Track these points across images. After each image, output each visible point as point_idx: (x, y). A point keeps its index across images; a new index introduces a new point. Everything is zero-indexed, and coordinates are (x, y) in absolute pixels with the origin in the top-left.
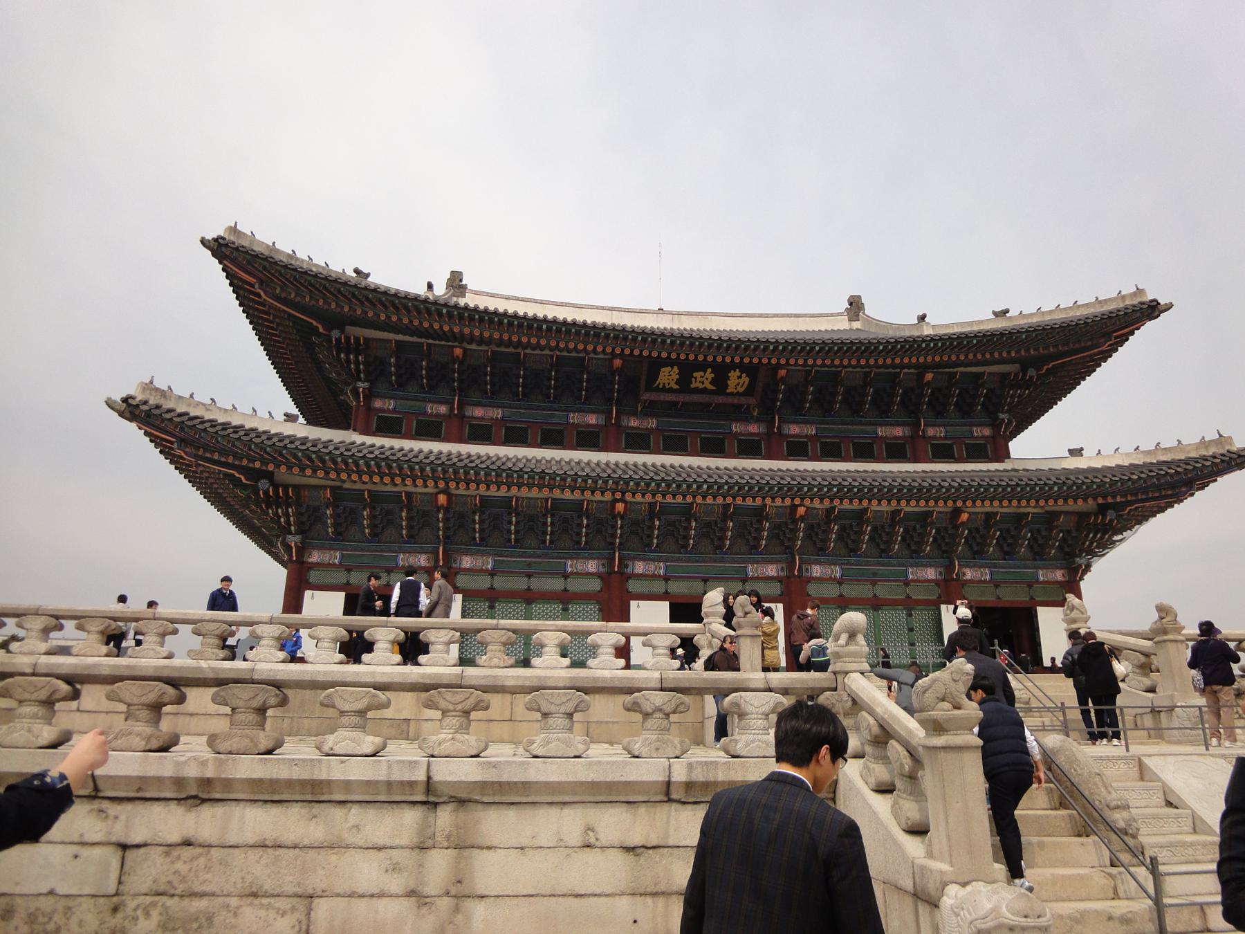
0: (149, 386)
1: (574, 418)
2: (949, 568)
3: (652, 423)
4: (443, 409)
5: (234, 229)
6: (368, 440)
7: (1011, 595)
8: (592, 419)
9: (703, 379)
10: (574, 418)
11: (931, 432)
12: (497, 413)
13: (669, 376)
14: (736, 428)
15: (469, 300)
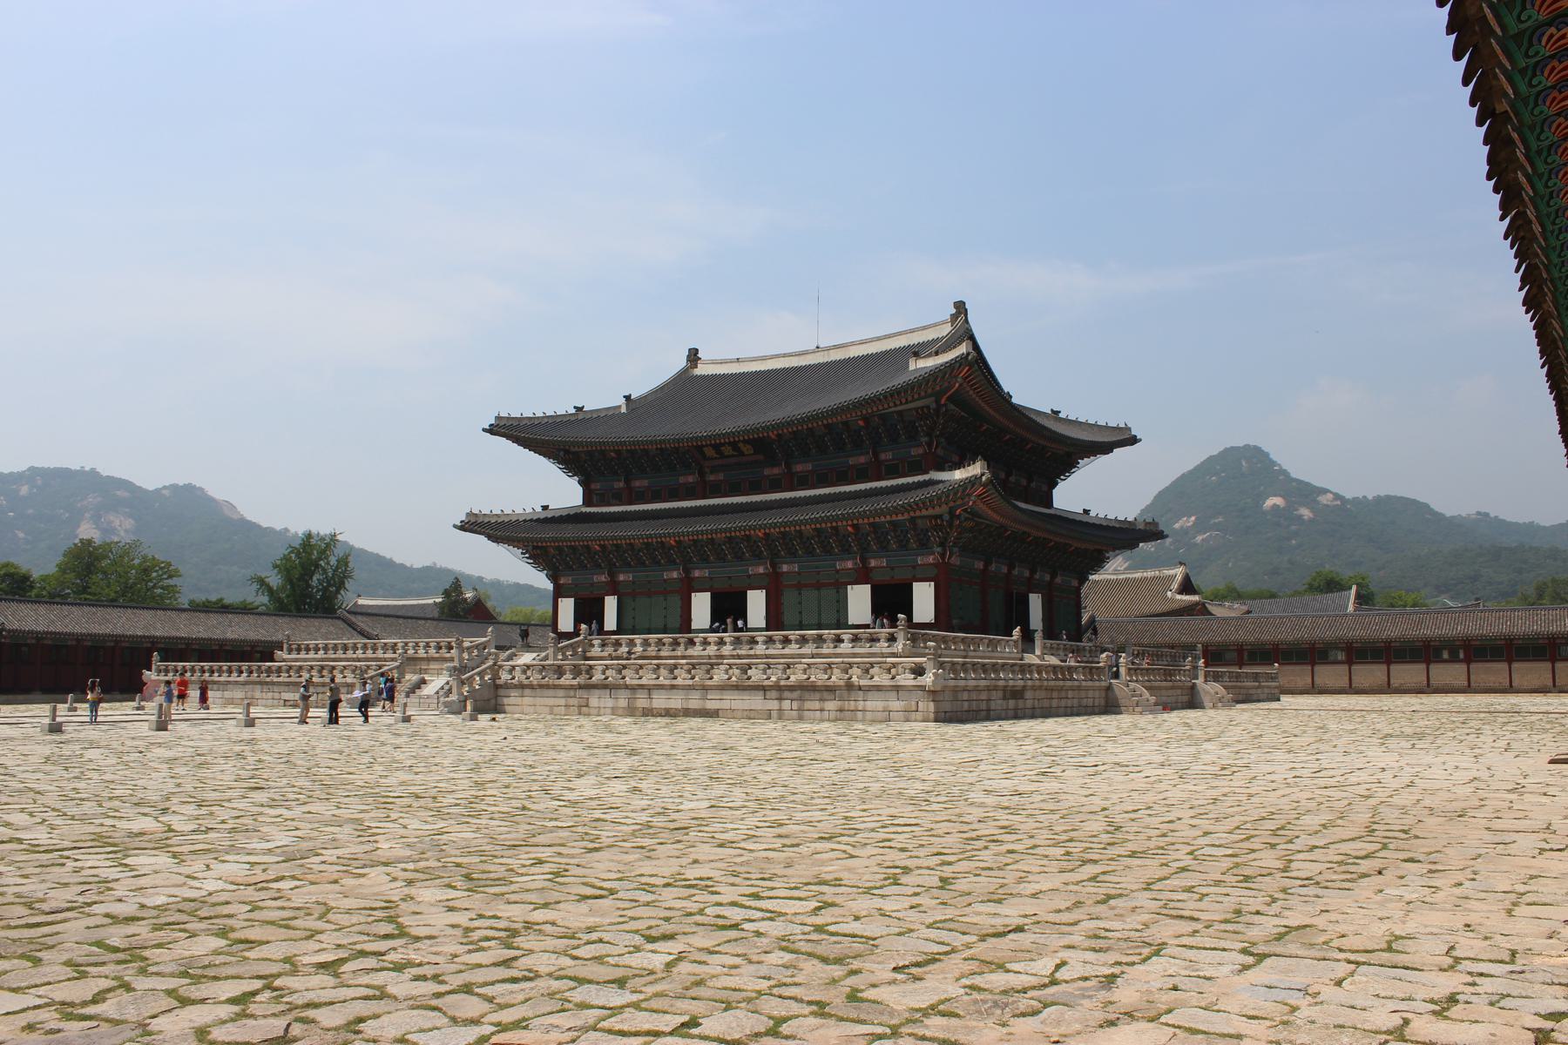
0: (470, 514)
1: (682, 480)
2: (864, 560)
3: (721, 476)
4: (621, 485)
5: (498, 418)
6: (588, 510)
7: (900, 575)
8: (690, 479)
9: (728, 450)
10: (682, 480)
11: (883, 456)
12: (645, 483)
13: (710, 452)
14: (767, 472)
15: (701, 370)
